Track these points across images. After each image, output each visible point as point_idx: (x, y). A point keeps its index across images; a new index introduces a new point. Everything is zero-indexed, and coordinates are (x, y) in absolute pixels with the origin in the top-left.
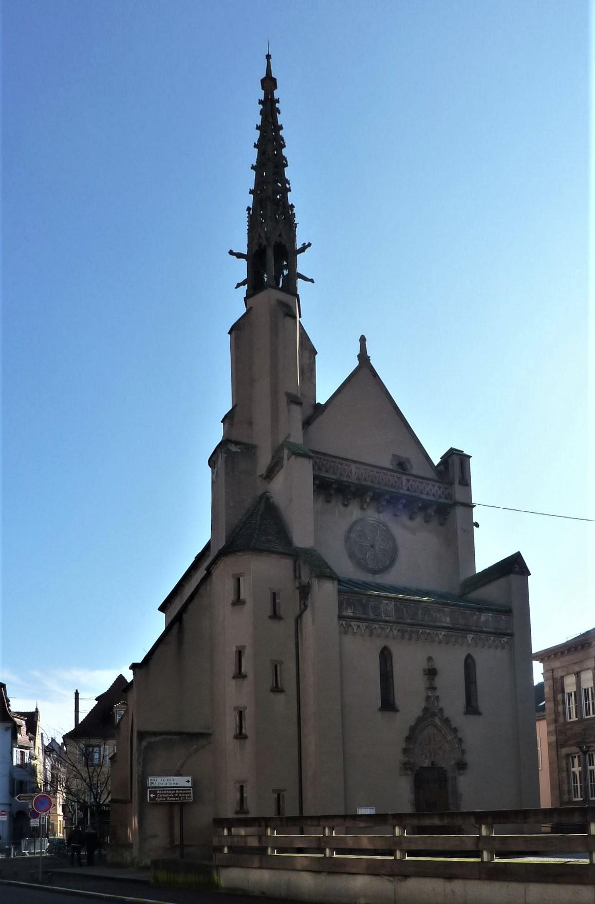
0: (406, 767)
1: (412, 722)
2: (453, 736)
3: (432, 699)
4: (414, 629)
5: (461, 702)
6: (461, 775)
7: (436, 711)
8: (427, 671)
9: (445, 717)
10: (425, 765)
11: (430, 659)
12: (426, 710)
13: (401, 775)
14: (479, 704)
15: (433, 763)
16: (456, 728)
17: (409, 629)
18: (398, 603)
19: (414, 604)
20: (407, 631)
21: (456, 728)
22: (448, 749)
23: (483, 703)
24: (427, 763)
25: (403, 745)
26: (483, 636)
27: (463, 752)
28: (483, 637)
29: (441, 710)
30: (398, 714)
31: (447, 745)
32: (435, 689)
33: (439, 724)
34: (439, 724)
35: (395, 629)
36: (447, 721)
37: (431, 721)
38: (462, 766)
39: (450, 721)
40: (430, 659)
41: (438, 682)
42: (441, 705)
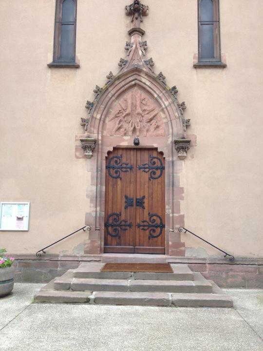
0: (89, 146)
1: (102, 84)
2: (170, 100)
3: (134, 46)
5: (191, 50)
6: (182, 158)
7: (141, 64)
8: (128, 8)
9: (157, 73)
12: (123, 63)
13: (77, 157)
14: (222, 52)
16: (174, 88)
21: (174, 88)
22: (165, 121)
23: (228, 52)
24: (127, 141)
27: (187, 124)
29: (150, 63)
30: (78, 71)
31: (163, 115)
32: (142, 33)
33: (148, 83)
34: (148, 83)
36: (160, 80)
37: (136, 79)
38: (183, 145)
39: (164, 78)
41: (147, 25)
42: (149, 56)
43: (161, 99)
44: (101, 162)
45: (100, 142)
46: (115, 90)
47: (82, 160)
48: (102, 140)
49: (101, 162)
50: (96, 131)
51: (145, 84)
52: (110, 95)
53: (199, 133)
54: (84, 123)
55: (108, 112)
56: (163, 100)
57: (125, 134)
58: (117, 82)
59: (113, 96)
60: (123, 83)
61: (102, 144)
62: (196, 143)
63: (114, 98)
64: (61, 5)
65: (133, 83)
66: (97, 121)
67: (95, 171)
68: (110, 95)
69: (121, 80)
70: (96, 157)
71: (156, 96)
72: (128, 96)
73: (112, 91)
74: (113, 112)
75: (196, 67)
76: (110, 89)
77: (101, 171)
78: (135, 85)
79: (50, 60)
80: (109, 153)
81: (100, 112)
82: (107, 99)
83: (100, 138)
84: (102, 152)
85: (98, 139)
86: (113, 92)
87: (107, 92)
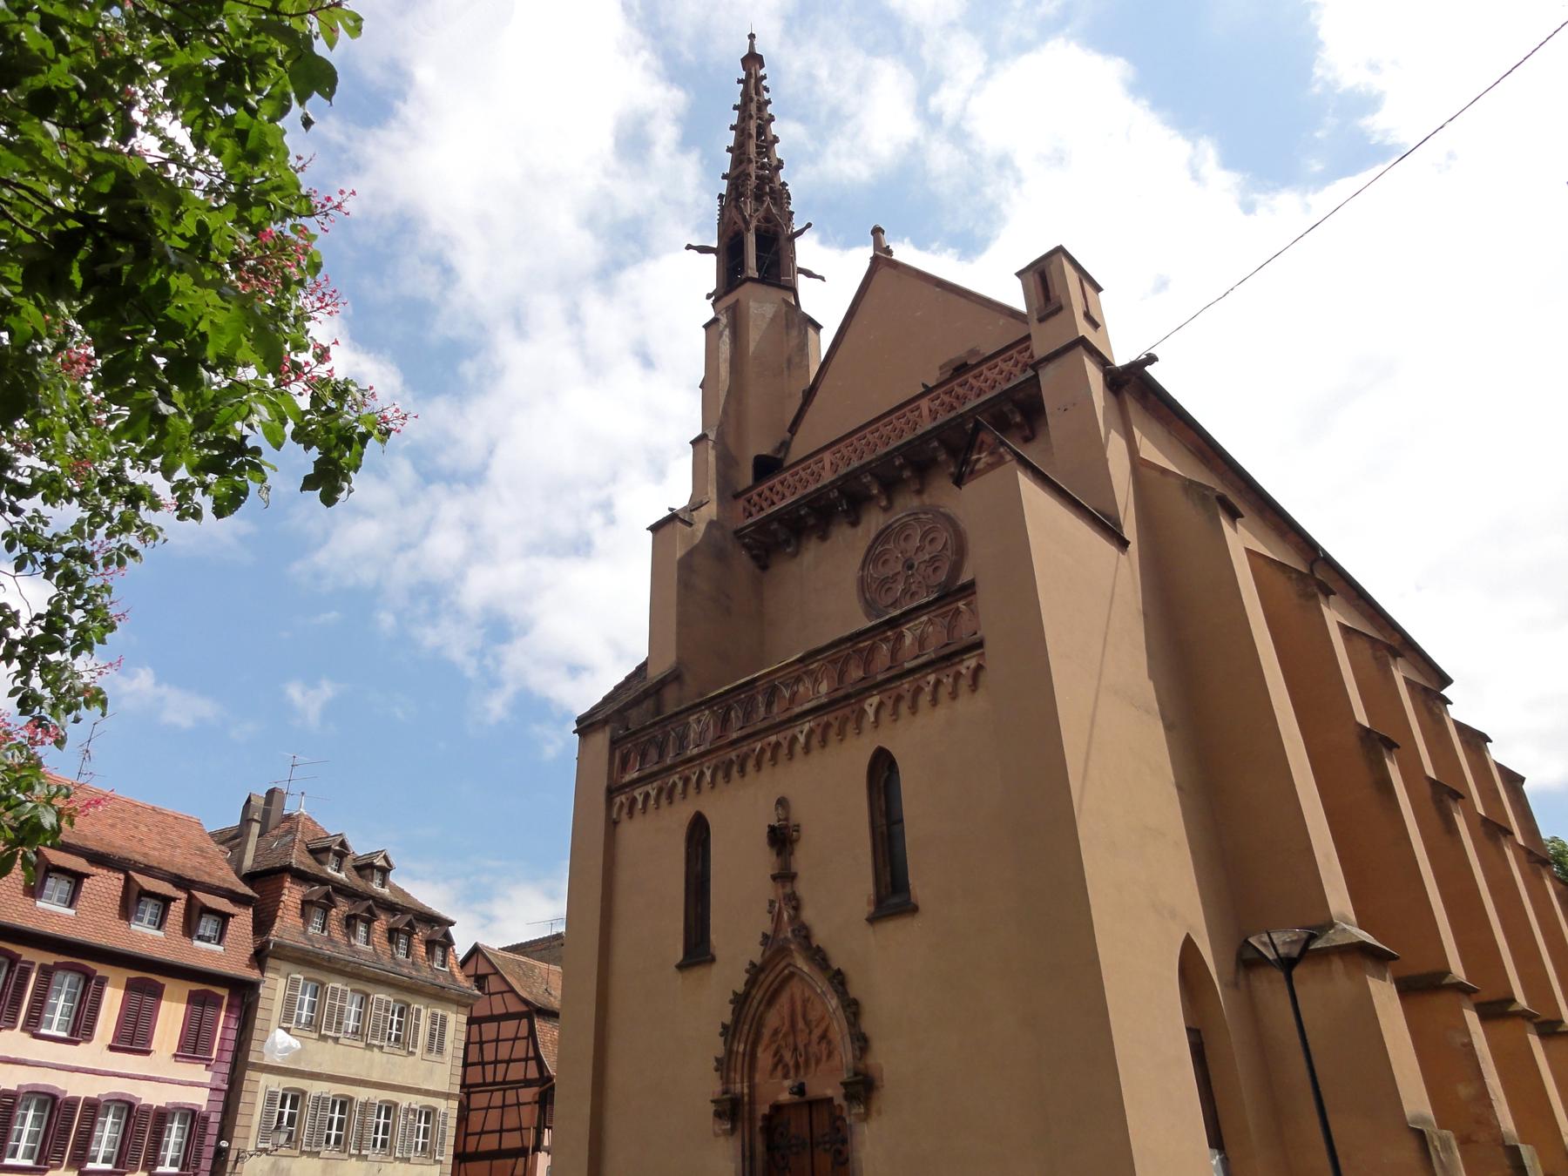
0: (730, 1110)
3: (777, 905)
4: (745, 749)
5: (862, 888)
10: (785, 1097)
11: (782, 803)
13: (716, 1135)
15: (800, 1090)
17: (733, 755)
18: (715, 708)
19: (743, 693)
20: (731, 761)
25: (718, 1048)
26: (906, 685)
28: (906, 686)
34: (806, 969)
35: (709, 768)
40: (782, 803)
41: (802, 859)
43: (826, 996)
44: (752, 1140)
45: (746, 1098)
46: (761, 993)
47: (722, 1140)
48: (751, 1094)
49: (752, 1140)
50: (738, 1080)
51: (801, 970)
52: (755, 1003)
53: (887, 1059)
54: (724, 1066)
55: (758, 1036)
56: (829, 997)
57: (786, 1076)
58: (762, 977)
59: (760, 1003)
60: (770, 978)
61: (752, 1102)
62: (882, 1081)
63: (762, 1008)
64: (700, 849)
65: (786, 972)
66: (740, 1058)
67: (740, 1159)
68: (755, 1003)
69: (767, 972)
70: (740, 1130)
71: (819, 991)
72: (784, 998)
73: (757, 994)
74: (767, 1033)
75: (872, 920)
76: (754, 992)
77: (752, 1158)
78: (792, 975)
79: (680, 956)
80: (765, 1117)
81: (743, 1038)
82: (752, 1011)
83: (746, 1091)
84: (752, 1119)
85: (743, 1093)
86: (758, 997)
87: (750, 1000)
